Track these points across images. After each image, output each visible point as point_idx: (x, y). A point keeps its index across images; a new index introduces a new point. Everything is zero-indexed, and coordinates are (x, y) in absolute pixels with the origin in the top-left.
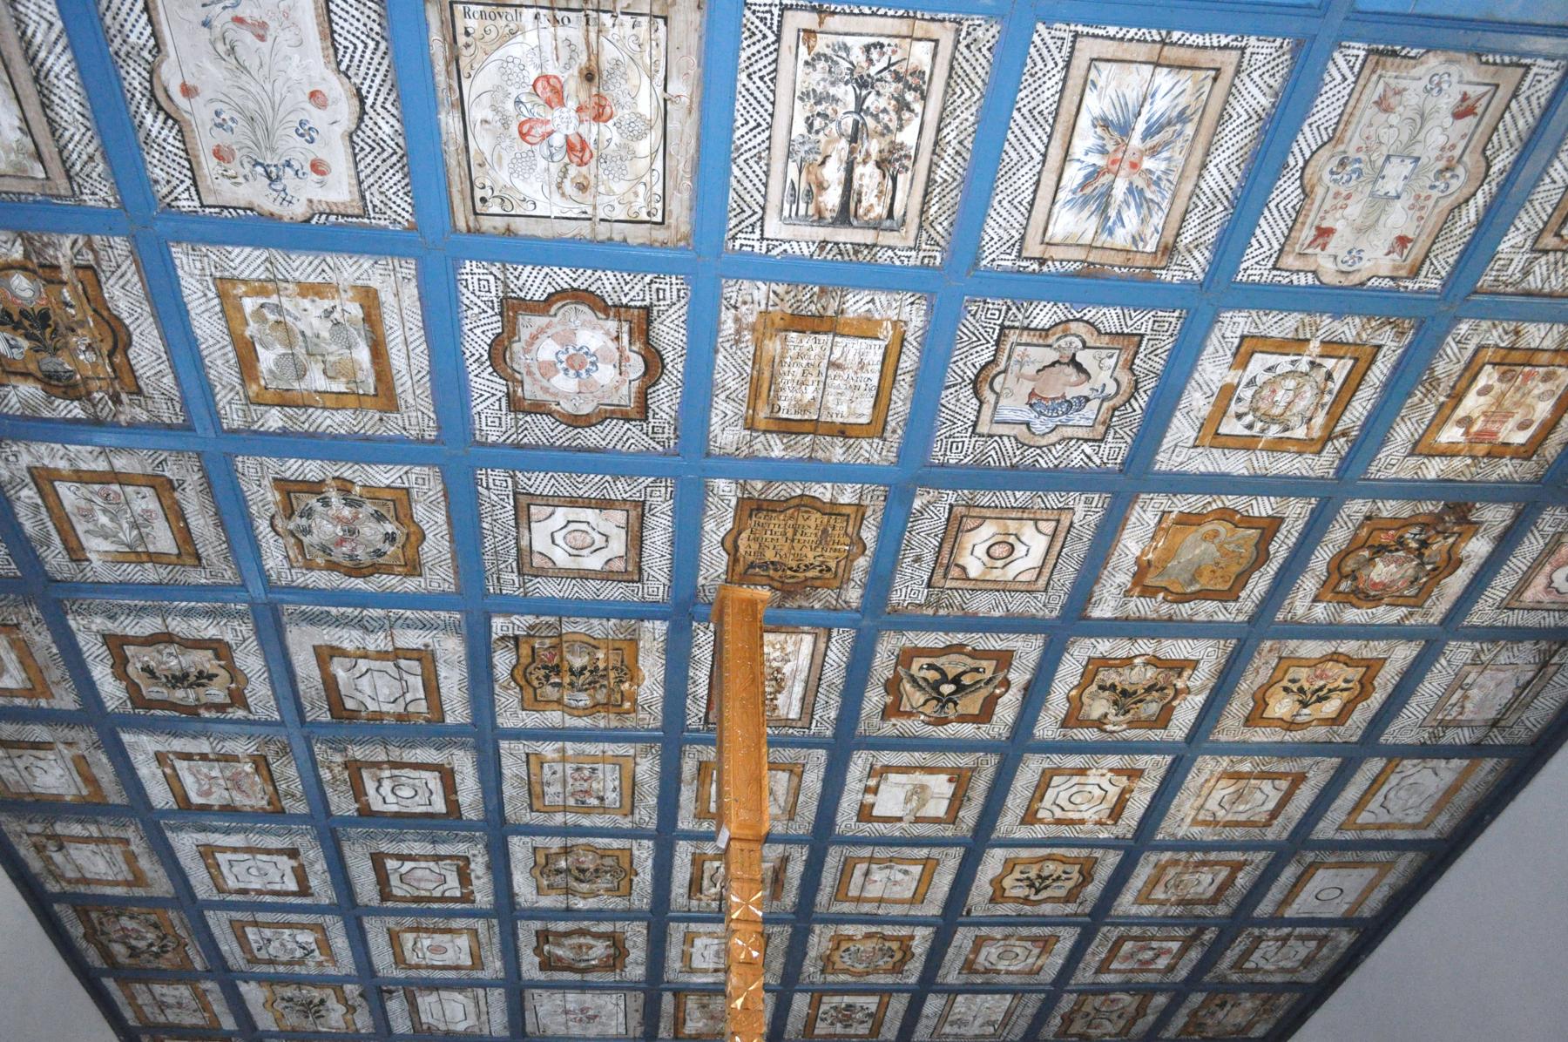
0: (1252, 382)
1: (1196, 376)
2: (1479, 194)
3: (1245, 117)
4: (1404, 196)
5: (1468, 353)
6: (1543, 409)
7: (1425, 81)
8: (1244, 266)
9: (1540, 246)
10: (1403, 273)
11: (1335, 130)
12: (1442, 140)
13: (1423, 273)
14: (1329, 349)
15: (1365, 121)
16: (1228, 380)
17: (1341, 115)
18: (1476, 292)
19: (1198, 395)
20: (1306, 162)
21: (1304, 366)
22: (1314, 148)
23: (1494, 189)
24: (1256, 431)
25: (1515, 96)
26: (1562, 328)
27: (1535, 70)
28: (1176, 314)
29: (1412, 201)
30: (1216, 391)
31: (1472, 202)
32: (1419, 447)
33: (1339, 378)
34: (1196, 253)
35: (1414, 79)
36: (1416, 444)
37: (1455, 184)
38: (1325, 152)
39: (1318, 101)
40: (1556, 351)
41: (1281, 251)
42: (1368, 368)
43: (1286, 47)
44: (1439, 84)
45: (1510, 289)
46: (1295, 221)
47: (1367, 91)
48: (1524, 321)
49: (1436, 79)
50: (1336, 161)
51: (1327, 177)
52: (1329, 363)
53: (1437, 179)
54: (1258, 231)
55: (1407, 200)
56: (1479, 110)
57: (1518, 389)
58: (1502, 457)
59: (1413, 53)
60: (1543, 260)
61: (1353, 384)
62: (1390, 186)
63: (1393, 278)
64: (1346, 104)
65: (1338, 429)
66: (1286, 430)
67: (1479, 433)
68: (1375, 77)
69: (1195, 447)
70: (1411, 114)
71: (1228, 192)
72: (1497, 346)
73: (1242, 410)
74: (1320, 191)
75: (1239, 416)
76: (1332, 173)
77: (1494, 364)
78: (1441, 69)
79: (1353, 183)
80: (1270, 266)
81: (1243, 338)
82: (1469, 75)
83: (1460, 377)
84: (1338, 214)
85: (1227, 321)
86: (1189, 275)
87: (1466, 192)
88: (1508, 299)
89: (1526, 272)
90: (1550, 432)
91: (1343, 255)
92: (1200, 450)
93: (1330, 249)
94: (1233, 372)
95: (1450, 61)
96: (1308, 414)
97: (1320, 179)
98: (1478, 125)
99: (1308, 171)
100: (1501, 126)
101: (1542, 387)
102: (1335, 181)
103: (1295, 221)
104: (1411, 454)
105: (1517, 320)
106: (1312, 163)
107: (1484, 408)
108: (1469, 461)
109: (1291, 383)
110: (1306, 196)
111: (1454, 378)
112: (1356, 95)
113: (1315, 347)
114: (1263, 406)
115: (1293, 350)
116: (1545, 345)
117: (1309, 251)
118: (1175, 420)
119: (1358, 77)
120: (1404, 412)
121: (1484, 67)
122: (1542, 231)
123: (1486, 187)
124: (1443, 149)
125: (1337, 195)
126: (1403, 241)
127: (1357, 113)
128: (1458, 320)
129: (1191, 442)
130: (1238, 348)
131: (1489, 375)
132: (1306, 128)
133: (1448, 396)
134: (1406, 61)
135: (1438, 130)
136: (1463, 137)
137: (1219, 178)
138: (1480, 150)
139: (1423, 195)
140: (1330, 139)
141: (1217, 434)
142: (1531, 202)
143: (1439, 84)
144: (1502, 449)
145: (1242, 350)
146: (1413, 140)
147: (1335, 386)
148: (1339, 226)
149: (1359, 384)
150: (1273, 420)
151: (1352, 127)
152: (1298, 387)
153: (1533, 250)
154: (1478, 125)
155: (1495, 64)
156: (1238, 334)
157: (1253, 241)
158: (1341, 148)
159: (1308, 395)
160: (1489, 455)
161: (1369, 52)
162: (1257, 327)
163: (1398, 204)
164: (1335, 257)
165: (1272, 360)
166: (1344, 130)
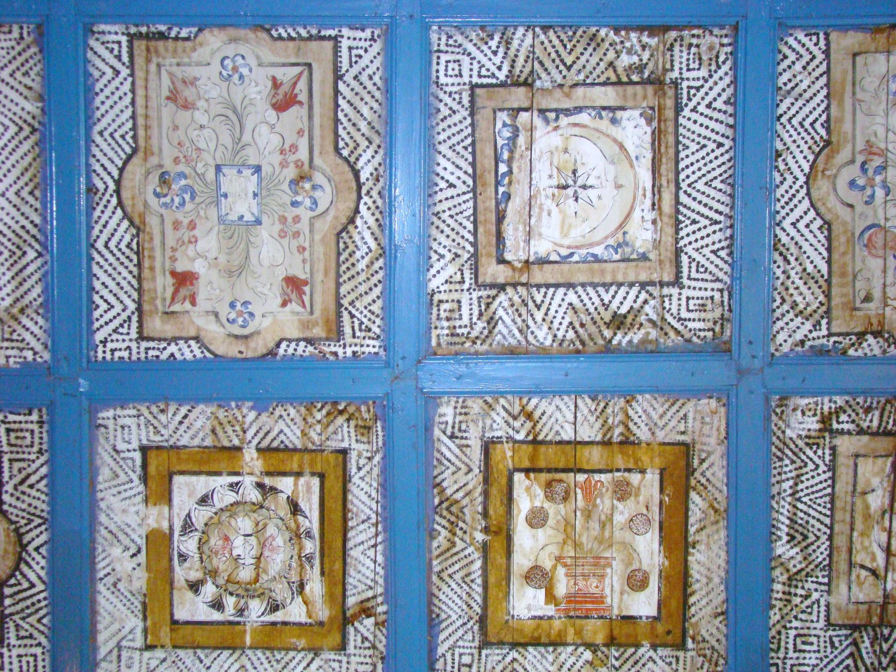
0: (188, 526)
1: (103, 518)
2: (362, 208)
3: (13, 129)
4: (264, 219)
5: (476, 454)
7: (216, 66)
8: (99, 336)
11: (134, 137)
12: (276, 140)
13: (347, 330)
14: (275, 460)
15: (166, 122)
16: (152, 523)
17: (133, 117)
19: (117, 551)
20: (118, 183)
21: (254, 495)
22: (120, 164)
24: (229, 613)
25: (338, 77)
27: (345, 44)
28: (35, 417)
29: (278, 227)
30: (142, 542)
31: (359, 222)
32: (491, 629)
33: (311, 505)
34: (25, 321)
35: (199, 64)
36: (483, 621)
38: (136, 169)
39: (97, 102)
40: (606, 443)
41: (139, 309)
42: (345, 491)
43: (28, 39)
44: (235, 69)
46: (139, 265)
47: (152, 85)
48: (531, 393)
50: (154, 179)
51: (153, 201)
52: (286, 484)
53: (296, 193)
54: (97, 285)
56: (303, 97)
58: (638, 646)
60: (502, 297)
61: (337, 516)
63: (310, 341)
64: (133, 103)
65: (351, 601)
66: (275, 608)
67: (571, 598)
68: (153, 68)
69: (149, 647)
70: (220, 109)
71: (34, 231)
72: (510, 439)
73: (195, 575)
74: (153, 222)
75: (195, 587)
76: (157, 195)
77: (527, 471)
78: (230, 51)
79: (189, 206)
80: (134, 335)
81: (144, 450)
82: (268, 56)
83: (486, 494)
85: (110, 423)
86: (29, 355)
90: (686, 596)
91: (224, 310)
92: (160, 654)
94: (153, 511)
95: (233, 40)
96: (295, 578)
98: (310, 117)
99: (125, 194)
100: (341, 115)
101: (623, 512)
102: (165, 205)
103: (139, 265)
104: (485, 644)
106: (125, 183)
107: (554, 550)
108: (588, 655)
109: (245, 524)
110: (138, 229)
112: (140, 92)
113: (250, 454)
114: (221, 563)
115: (222, 466)
116: (587, 433)
118: (101, 599)
119: (132, 66)
120: (436, 566)
121: (279, 44)
122: (475, 256)
123: (366, 199)
126: (294, 284)
127: (153, 114)
129: (139, 642)
130: (145, 466)
131: (528, 489)
132: (98, 139)
133: (486, 530)
134: (180, 43)
135: (264, 129)
136: (300, 133)
137: (14, 212)
138: (331, 149)
140: (135, 151)
141: (175, 622)
143: (235, 69)
144: (627, 629)
145: (152, 470)
146: (239, 145)
147: (311, 520)
148: (199, 267)
149: (345, 520)
150: (249, 590)
151: (154, 132)
152: (259, 530)
154: (310, 117)
155: (291, 38)
156: (135, 444)
157: (96, 298)
158: (154, 160)
159: (279, 541)
160: (611, 641)
161: (132, 38)
162: (157, 432)
164: (216, 315)
165: (202, 484)
166: (148, 138)
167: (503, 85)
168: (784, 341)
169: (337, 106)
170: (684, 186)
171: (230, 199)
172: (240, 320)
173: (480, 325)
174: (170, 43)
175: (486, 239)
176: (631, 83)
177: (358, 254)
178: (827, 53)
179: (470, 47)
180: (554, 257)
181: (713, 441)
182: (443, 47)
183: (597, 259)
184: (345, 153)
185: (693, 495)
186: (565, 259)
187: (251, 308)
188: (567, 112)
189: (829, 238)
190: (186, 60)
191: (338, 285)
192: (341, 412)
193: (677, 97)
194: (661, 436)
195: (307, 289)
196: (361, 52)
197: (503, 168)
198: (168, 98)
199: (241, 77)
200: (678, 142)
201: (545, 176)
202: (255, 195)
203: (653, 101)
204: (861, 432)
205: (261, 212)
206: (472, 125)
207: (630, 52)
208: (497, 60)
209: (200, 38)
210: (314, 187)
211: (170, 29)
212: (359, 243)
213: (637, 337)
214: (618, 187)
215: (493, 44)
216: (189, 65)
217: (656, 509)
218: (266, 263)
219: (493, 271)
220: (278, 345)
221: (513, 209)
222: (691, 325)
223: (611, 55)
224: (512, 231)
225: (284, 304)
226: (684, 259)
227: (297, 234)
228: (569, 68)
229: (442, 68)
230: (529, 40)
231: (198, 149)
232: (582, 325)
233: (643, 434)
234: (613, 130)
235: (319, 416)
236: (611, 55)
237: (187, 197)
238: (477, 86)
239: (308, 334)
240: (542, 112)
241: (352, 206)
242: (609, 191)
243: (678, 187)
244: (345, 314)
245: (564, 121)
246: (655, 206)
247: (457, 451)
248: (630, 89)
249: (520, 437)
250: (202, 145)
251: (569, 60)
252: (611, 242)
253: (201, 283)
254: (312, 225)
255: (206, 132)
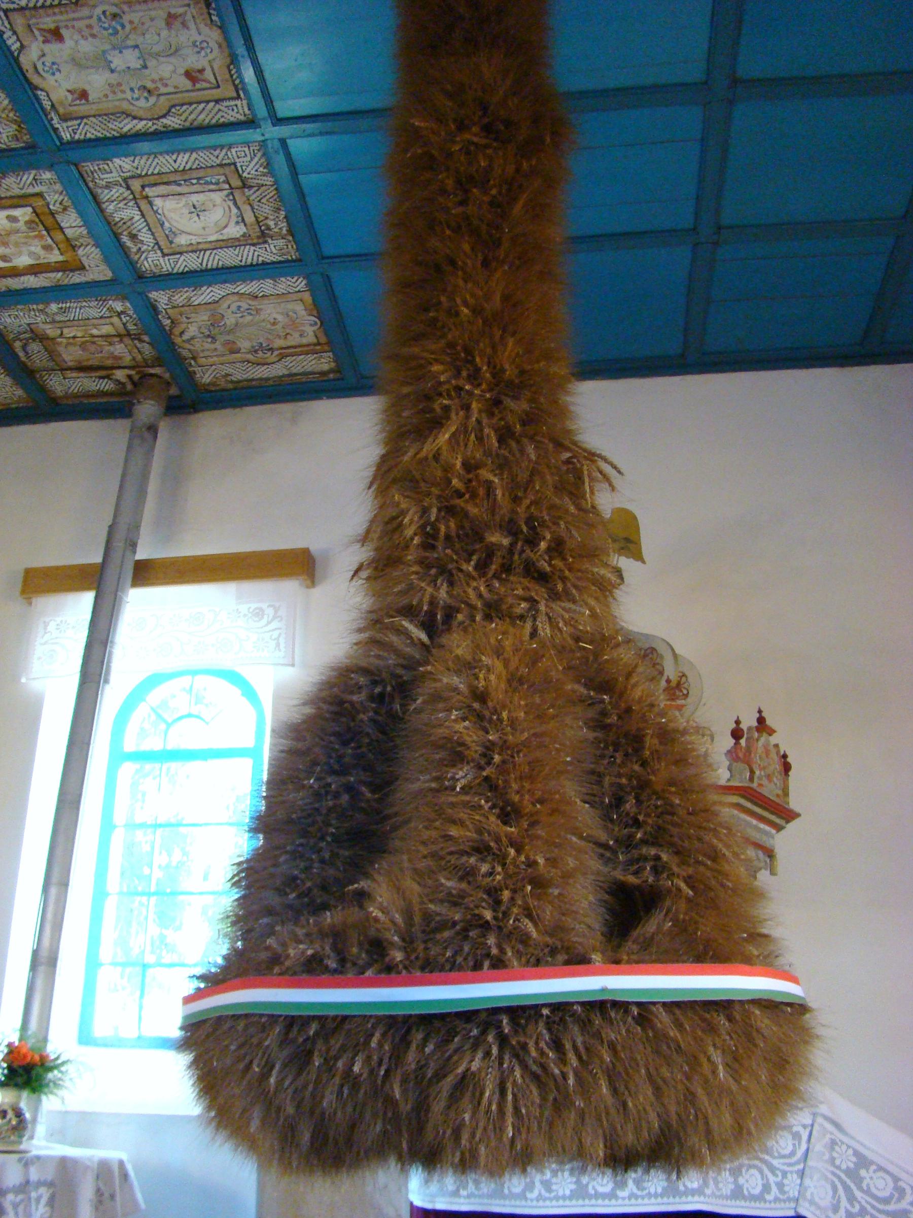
2: (144, 122)
4: (115, 75)
5: (31, 190)
6: (23, 261)
7: (199, 39)
9: (130, 182)
10: (61, 111)
12: (166, 75)
13: (69, 123)
15: (153, 13)
18: (76, 165)
23: (151, 130)
25: (217, 101)
26: (85, 232)
27: (238, 102)
29: (115, 83)
31: (135, 121)
35: (198, 29)
37: (142, 103)
40: (68, 240)
44: (202, 48)
45: (91, 185)
48: (76, 208)
49: (205, 45)
50: (114, 10)
55: (114, 78)
56: (198, 86)
57: (26, 237)
59: (214, 18)
60: (122, 190)
62: (118, 61)
63: (53, 106)
72: (48, 205)
76: (104, 12)
77: (35, 212)
79: (105, 33)
83: (12, 197)
84: (76, 37)
87: (141, 113)
88: (85, 188)
89: (108, 186)
90: (10, 276)
91: (48, 60)
93: (47, 48)
95: (220, 46)
97: (95, 6)
98: (187, 91)
105: (73, 203)
111: (9, 194)
116: (67, 231)
117: (37, 33)
121: (227, 72)
122: (140, 176)
123: (150, 123)
124: (161, 79)
125: (89, 27)
126: (84, 95)
128: (51, 167)
131: (25, 213)
134: (207, 16)
135: (171, 68)
136: (175, 87)
138: (172, 103)
139: (123, 88)
142: (156, 157)
148: (69, 43)
153: (125, 180)
154: (187, 91)
155: (232, 76)
158: (125, 8)
163: (107, 74)
167: (240, 176)
168: (153, 295)
169: (200, 103)
170: (215, 251)
171: (120, 55)
172: (46, 69)
173: (104, 183)
174: (205, 11)
175: (152, 179)
176: (260, 227)
177: (117, 123)
178: (299, 291)
179: (256, 159)
180: (155, 208)
181: (92, 277)
182: (251, 149)
183: (162, 225)
184: (173, 110)
185: (60, 274)
186: (156, 212)
187: (57, 74)
188: (235, 204)
189: (210, 303)
190: (198, 21)
191: (94, 116)
192: (19, 126)
193: (259, 244)
194: (84, 259)
195: (83, 101)
196: (236, 110)
197: (194, 181)
198: (169, 13)
199: (199, 52)
200: (236, 246)
201: (198, 199)
202: (129, 68)
203: (253, 235)
204: (124, 324)
205: (119, 72)
206: (212, 166)
207: (276, 224)
208: (253, 172)
209: (215, 28)
210: (146, 98)
211: (214, 9)
212: (123, 123)
213: (129, 244)
214: (204, 228)
215: (261, 169)
216: (195, 24)
217: (46, 261)
218: (89, 78)
219: (136, 185)
220: (42, 90)
221: (174, 188)
222: (145, 262)
223: (272, 217)
224: (162, 189)
225: (69, 91)
226: (178, 256)
227: (114, 93)
228: (259, 201)
229: (240, 149)
230: (268, 183)
231: (144, 34)
232: (124, 223)
233: (81, 252)
234: (232, 223)
235: (11, 115)
236: (272, 217)
237: (111, 31)
238: (236, 166)
239: (57, 106)
240: (232, 194)
241: (144, 117)
242: (202, 225)
243: (213, 249)
244: (78, 122)
245: (231, 204)
246: (199, 243)
247: (28, 182)
248: (257, 227)
249: (51, 207)
250: (147, 36)
251: (264, 201)
252: (174, 230)
253: (59, 46)
254: (123, 99)
255: (156, 38)
